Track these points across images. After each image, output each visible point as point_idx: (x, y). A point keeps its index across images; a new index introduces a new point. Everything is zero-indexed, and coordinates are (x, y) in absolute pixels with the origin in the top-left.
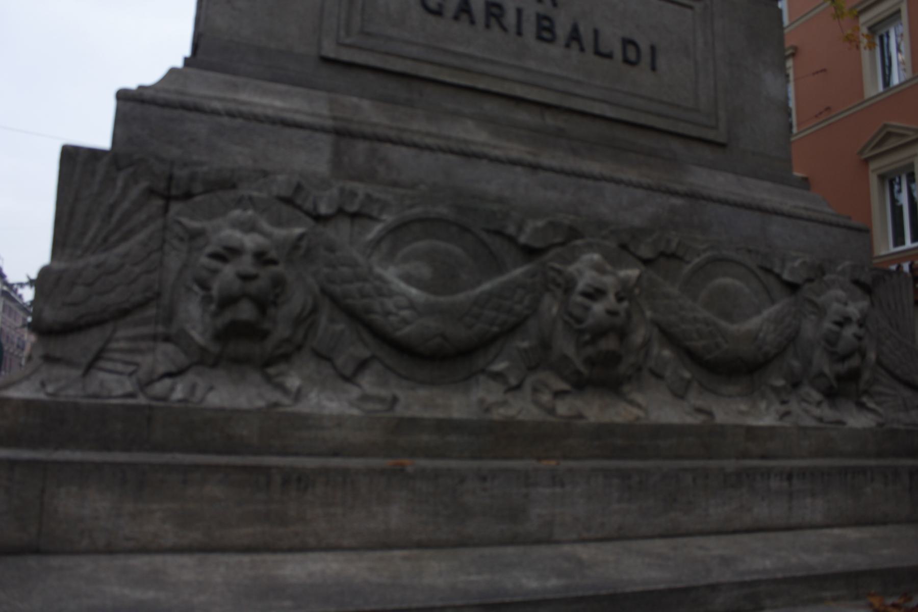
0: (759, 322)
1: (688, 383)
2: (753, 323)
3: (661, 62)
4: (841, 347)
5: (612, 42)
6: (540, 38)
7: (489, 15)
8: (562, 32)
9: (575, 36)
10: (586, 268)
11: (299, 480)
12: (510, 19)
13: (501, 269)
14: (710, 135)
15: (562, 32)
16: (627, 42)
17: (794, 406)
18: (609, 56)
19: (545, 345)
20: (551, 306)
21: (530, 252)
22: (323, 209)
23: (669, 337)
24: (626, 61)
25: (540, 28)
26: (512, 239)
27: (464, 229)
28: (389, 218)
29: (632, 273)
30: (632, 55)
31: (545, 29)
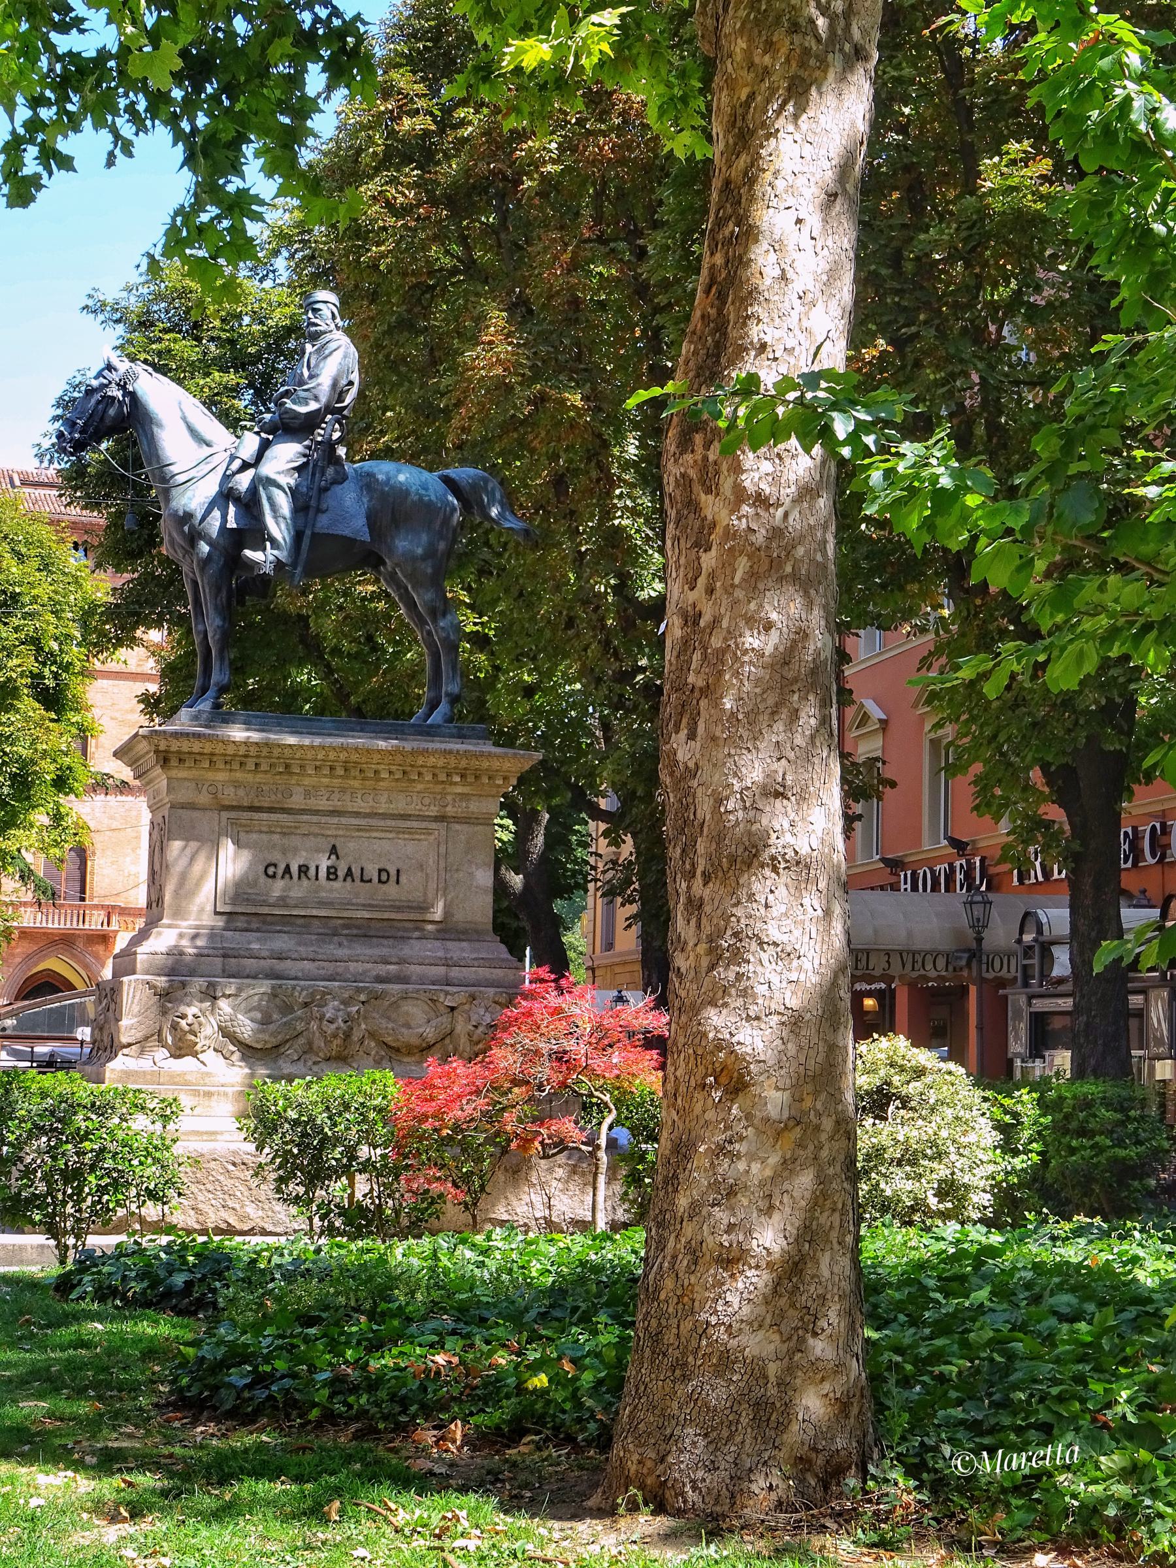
1: (382, 1058)
3: (403, 879)
4: (475, 1038)
5: (372, 872)
8: (341, 873)
9: (349, 873)
11: (209, 1094)
12: (312, 872)
15: (341, 873)
19: (310, 1044)
25: (329, 873)
30: (384, 877)
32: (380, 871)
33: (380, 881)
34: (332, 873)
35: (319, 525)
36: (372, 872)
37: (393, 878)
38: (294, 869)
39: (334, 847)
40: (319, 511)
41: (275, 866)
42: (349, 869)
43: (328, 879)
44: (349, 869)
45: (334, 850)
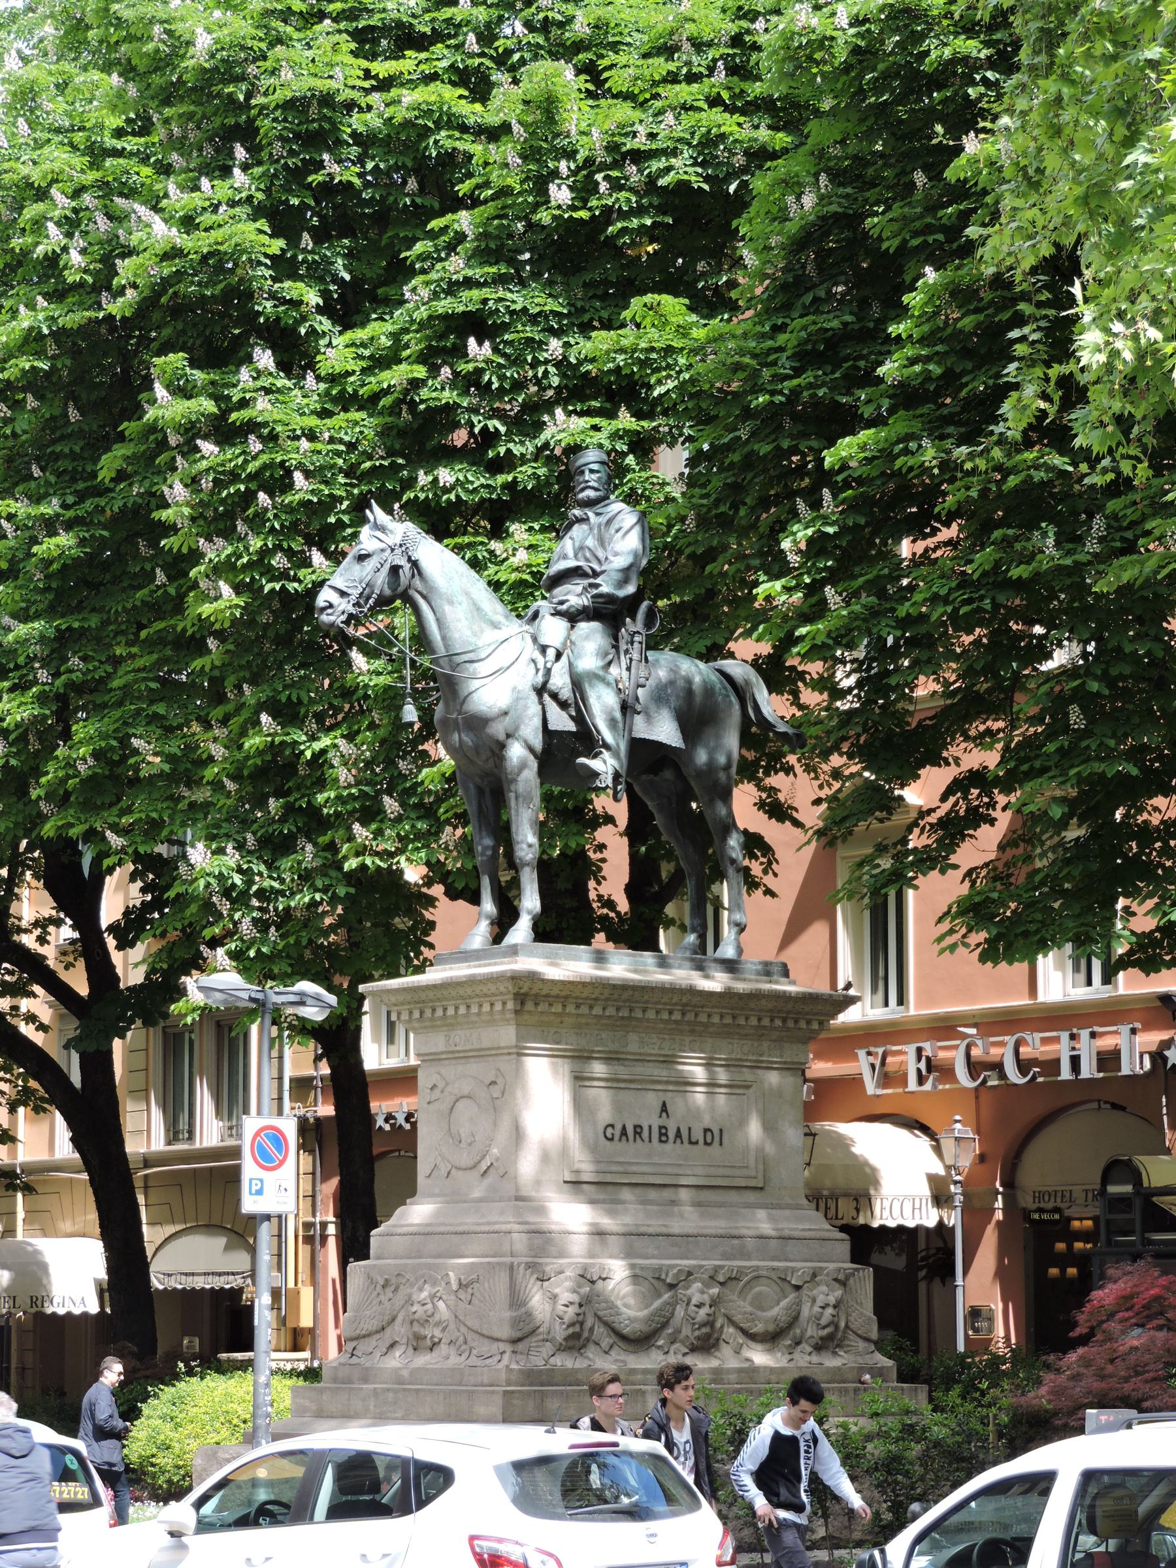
0: (778, 1311)
2: (775, 1311)
5: (698, 1135)
8: (672, 1134)
9: (678, 1134)
10: (695, 1292)
12: (645, 1134)
13: (659, 1296)
14: (753, 1183)
15: (672, 1134)
16: (706, 1130)
17: (797, 1355)
20: (680, 1312)
21: (672, 1286)
23: (731, 1322)
29: (715, 1291)
31: (663, 1133)
34: (663, 1133)
36: (698, 1135)
38: (630, 1131)
45: (664, 1108)
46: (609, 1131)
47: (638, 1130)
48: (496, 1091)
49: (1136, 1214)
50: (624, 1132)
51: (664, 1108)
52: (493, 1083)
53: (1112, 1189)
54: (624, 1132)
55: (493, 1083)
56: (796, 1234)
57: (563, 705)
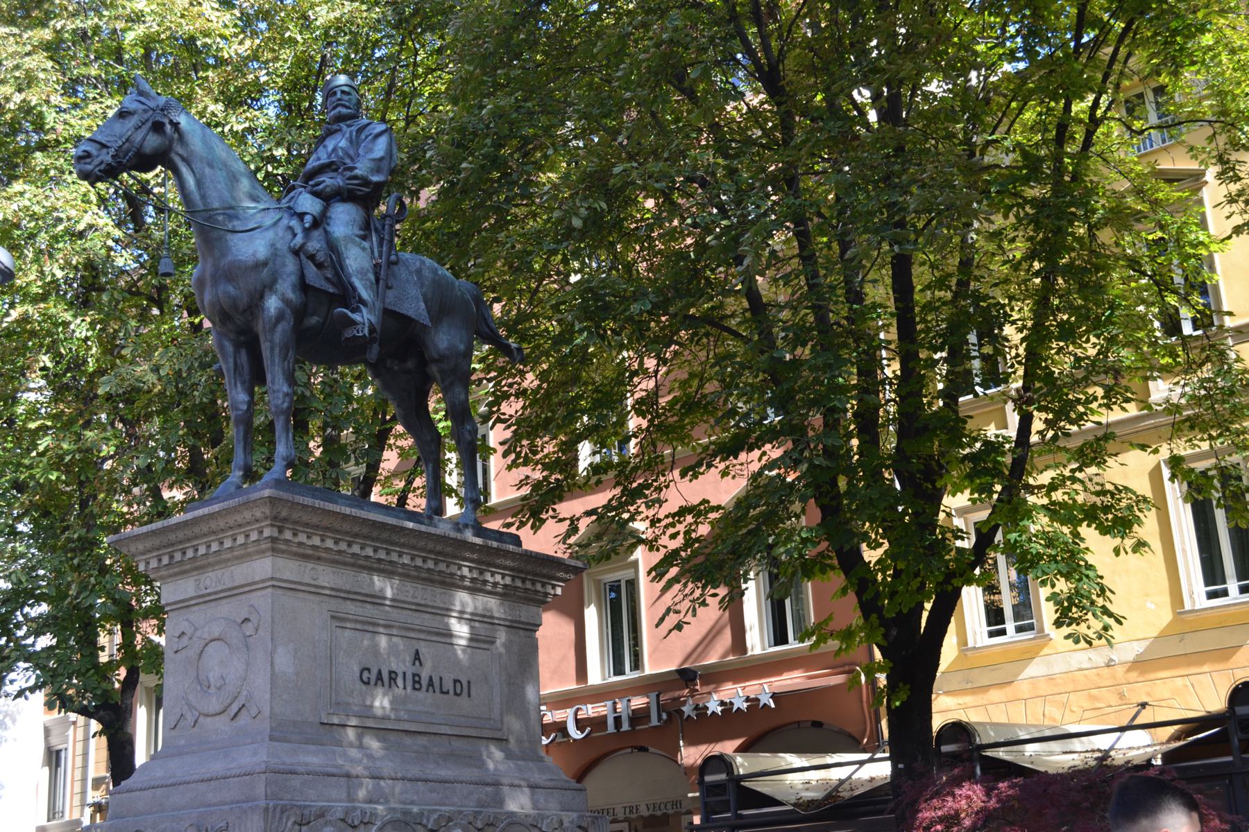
5: (448, 685)
6: (414, 689)
7: (391, 678)
8: (424, 682)
9: (431, 683)
15: (424, 682)
16: (456, 681)
18: (447, 693)
22: (356, 823)
24: (456, 694)
25: (414, 682)
26: (425, 826)
27: (407, 824)
28: (379, 823)
32: (456, 681)
33: (456, 694)
35: (387, 301)
36: (448, 685)
37: (465, 691)
39: (417, 652)
40: (389, 287)
41: (369, 670)
42: (431, 678)
43: (414, 689)
44: (431, 678)
45: (417, 657)
46: (366, 674)
47: (393, 675)
48: (249, 629)
49: (731, 796)
50: (379, 677)
51: (417, 657)
52: (246, 620)
53: (708, 778)
54: (379, 677)
55: (246, 620)
56: (542, 783)
57: (320, 266)
